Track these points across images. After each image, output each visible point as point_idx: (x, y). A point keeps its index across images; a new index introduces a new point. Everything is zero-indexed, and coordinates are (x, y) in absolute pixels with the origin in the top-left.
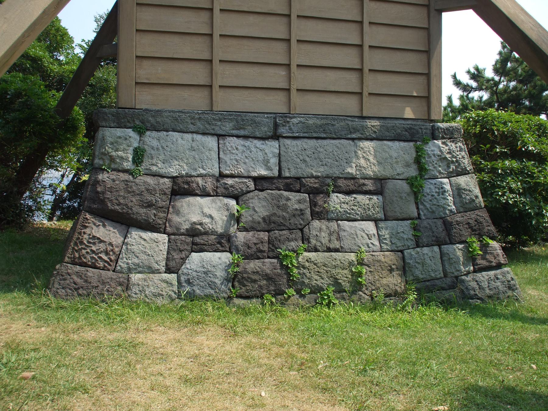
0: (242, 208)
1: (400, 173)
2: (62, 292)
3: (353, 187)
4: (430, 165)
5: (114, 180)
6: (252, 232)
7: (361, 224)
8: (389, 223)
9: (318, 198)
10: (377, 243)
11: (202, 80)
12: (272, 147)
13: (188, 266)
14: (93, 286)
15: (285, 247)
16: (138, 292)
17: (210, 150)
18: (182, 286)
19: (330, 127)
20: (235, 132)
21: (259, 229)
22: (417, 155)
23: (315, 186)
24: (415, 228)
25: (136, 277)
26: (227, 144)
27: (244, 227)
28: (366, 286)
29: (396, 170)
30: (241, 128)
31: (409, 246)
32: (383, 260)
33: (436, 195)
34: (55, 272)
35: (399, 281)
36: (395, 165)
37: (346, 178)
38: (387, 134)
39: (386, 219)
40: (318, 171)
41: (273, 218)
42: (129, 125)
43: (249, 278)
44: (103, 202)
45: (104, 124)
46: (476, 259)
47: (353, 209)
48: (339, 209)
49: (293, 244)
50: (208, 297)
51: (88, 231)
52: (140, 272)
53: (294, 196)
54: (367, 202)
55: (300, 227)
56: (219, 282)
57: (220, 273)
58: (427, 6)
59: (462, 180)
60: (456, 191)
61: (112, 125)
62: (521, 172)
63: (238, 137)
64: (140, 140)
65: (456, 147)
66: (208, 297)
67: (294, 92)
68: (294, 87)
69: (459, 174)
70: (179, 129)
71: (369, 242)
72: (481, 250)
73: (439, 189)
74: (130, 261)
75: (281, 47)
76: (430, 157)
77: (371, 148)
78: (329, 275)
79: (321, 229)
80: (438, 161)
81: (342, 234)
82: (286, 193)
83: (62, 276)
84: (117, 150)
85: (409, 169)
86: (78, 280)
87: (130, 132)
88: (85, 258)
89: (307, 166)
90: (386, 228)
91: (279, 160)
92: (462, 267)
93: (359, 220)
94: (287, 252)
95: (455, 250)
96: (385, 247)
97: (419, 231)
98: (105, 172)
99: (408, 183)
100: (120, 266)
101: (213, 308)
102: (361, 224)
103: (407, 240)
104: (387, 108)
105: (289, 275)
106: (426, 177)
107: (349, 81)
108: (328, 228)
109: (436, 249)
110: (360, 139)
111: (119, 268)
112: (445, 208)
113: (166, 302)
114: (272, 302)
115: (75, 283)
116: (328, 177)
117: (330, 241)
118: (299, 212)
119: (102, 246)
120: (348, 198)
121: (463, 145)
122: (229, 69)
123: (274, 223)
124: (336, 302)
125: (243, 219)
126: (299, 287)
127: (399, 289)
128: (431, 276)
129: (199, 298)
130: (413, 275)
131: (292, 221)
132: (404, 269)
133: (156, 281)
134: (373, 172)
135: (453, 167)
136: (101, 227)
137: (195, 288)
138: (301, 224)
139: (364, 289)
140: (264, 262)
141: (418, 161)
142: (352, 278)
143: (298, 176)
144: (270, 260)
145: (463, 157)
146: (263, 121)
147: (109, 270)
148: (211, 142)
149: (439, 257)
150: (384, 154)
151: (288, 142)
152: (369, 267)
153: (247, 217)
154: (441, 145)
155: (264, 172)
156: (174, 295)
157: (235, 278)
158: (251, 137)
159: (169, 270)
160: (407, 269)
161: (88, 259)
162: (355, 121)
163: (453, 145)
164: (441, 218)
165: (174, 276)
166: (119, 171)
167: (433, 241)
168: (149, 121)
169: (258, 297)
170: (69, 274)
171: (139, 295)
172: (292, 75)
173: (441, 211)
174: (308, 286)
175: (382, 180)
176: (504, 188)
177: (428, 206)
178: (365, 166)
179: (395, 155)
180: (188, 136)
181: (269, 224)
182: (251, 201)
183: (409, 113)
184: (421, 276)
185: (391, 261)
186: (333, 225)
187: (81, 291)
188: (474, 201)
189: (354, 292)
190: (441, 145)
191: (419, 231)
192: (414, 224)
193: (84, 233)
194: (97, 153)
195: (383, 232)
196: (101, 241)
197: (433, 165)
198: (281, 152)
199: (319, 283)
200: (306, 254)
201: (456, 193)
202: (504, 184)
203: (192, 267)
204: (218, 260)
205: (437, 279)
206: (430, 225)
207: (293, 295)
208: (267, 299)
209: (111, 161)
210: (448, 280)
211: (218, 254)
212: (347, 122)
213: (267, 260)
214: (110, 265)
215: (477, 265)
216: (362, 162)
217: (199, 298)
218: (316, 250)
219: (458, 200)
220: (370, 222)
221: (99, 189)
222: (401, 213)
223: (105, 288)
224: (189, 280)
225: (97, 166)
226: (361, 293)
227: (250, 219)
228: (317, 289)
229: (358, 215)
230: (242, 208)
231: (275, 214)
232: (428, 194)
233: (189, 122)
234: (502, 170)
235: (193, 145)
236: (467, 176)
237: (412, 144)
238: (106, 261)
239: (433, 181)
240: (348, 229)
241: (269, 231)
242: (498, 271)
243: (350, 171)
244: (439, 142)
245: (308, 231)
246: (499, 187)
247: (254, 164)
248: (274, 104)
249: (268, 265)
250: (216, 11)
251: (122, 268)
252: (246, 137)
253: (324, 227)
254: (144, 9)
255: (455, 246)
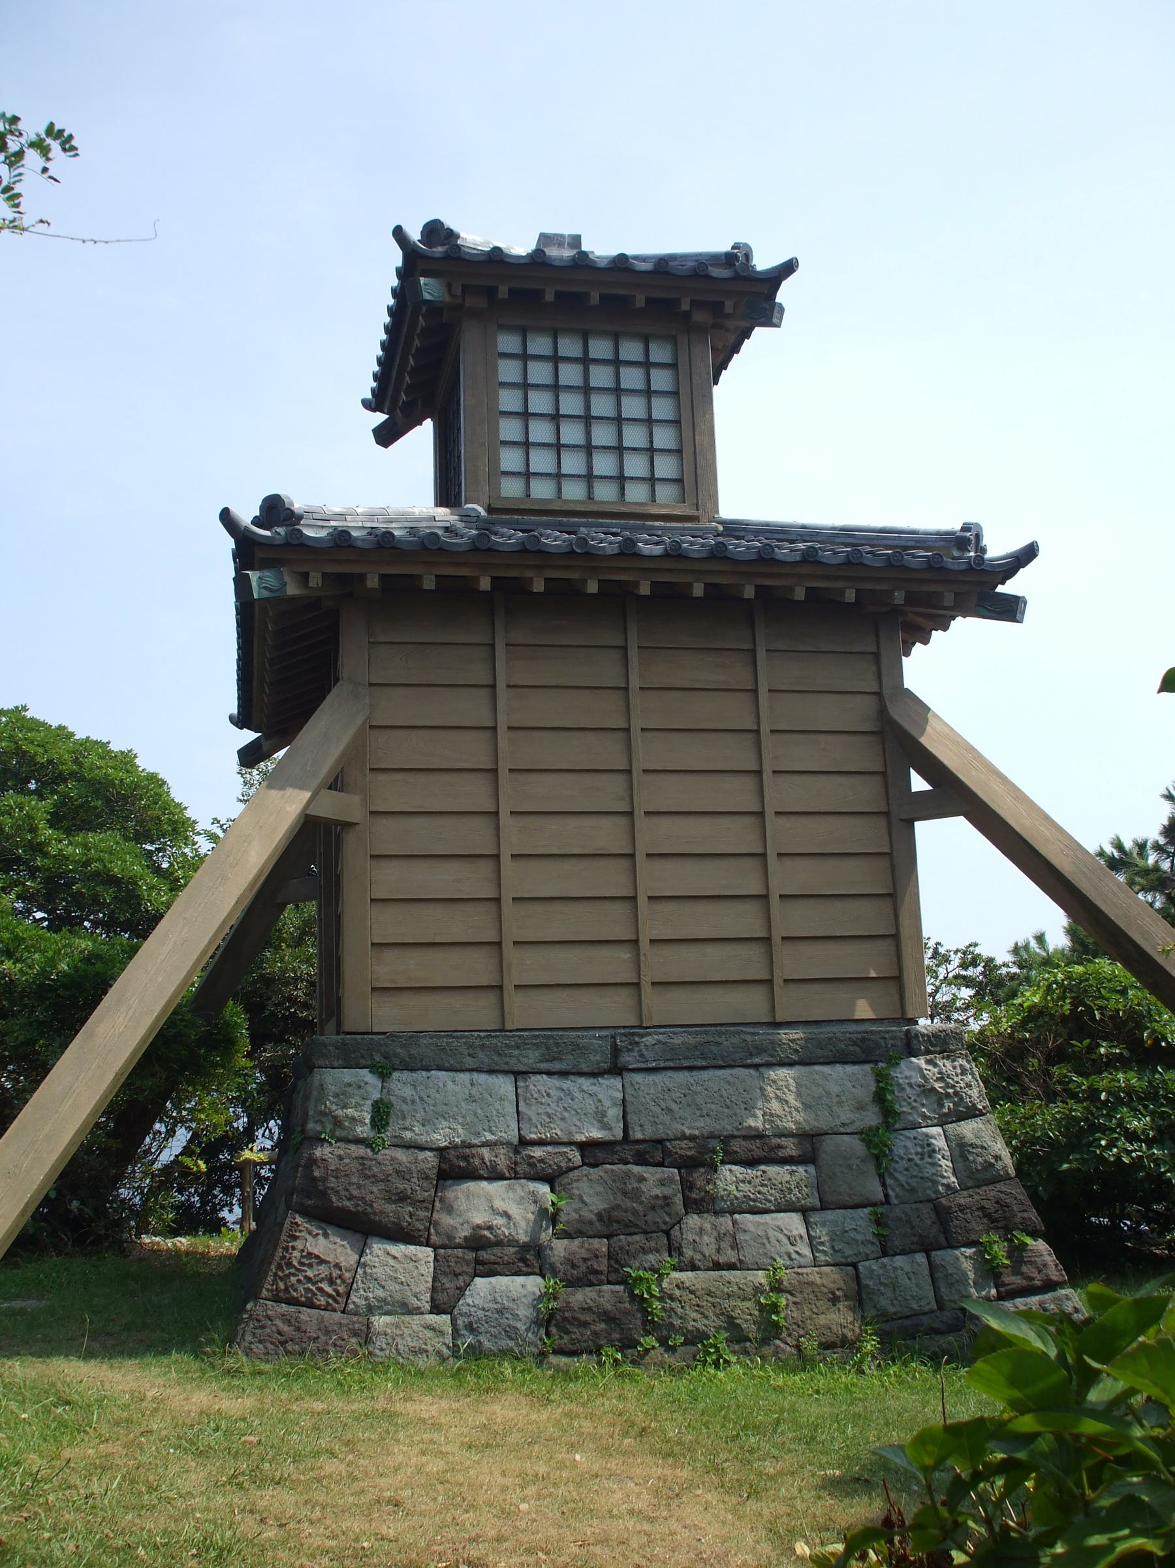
0: (560, 1199)
1: (847, 1121)
2: (258, 1348)
3: (760, 1151)
4: (904, 1103)
5: (341, 1158)
6: (580, 1240)
7: (776, 1219)
8: (829, 1215)
9: (695, 1176)
10: (806, 1251)
11: (486, 977)
12: (609, 1089)
13: (469, 1301)
14: (309, 1338)
15: (637, 1264)
16: (384, 1346)
17: (501, 1099)
18: (460, 1335)
19: (713, 1048)
20: (543, 1066)
21: (591, 1233)
22: (878, 1087)
23: (689, 1153)
24: (879, 1222)
25: (380, 1322)
26: (532, 1087)
27: (565, 1231)
28: (788, 1329)
29: (839, 1117)
30: (554, 1059)
31: (867, 1255)
32: (819, 1281)
33: (916, 1158)
34: (245, 1316)
35: (850, 1319)
36: (835, 1108)
37: (745, 1137)
38: (820, 1052)
39: (823, 1207)
40: (694, 1126)
41: (615, 1214)
42: (363, 1062)
43: (574, 1318)
44: (323, 1194)
45: (321, 1062)
46: (1001, 1273)
47: (759, 1192)
48: (735, 1193)
49: (652, 1258)
50: (504, 1353)
51: (299, 1244)
52: (387, 1313)
53: (652, 1174)
54: (787, 1177)
55: (664, 1227)
56: (523, 1328)
57: (525, 1312)
58: (887, 814)
59: (968, 1129)
60: (957, 1149)
61: (336, 1064)
62: (1151, 1095)
63: (550, 1073)
64: (383, 1087)
65: (954, 1068)
66: (504, 1353)
67: (646, 989)
68: (646, 980)
69: (962, 1117)
70: (447, 1065)
71: (791, 1249)
72: (1007, 1258)
73: (923, 1147)
74: (371, 1295)
75: (620, 910)
76: (904, 1089)
77: (791, 1081)
78: (718, 1311)
79: (701, 1230)
80: (918, 1096)
81: (741, 1237)
82: (637, 1169)
83: (259, 1321)
84: (345, 1106)
85: (864, 1113)
86: (285, 1328)
87: (366, 1075)
88: (296, 1290)
89: (674, 1118)
90: (823, 1224)
91: (624, 1112)
92: (973, 1290)
93: (773, 1212)
94: (641, 1273)
95: (957, 1258)
96: (821, 1257)
97: (887, 1226)
98: (326, 1145)
99: (863, 1140)
100: (354, 1303)
101: (514, 1370)
102: (776, 1219)
103: (863, 1243)
104: (819, 1004)
105: (645, 1312)
106: (897, 1126)
107: (749, 962)
108: (714, 1227)
109: (920, 1258)
110: (769, 1065)
111: (351, 1306)
112: (935, 1183)
113: (433, 1360)
114: (616, 1360)
115: (280, 1333)
116: (712, 1136)
117: (719, 1250)
118: (661, 1202)
119: (323, 1270)
120: (750, 1173)
121: (969, 1062)
122: (531, 957)
123: (617, 1222)
124: (733, 1359)
125: (563, 1217)
126: (665, 1333)
127: (849, 1334)
128: (912, 1309)
129: (489, 1355)
130: (875, 1307)
131: (649, 1217)
132: (859, 1296)
133: (415, 1327)
134: (796, 1122)
135: (948, 1105)
136: (320, 1237)
137: (482, 1338)
138: (665, 1223)
139: (784, 1335)
140: (600, 1291)
141: (880, 1098)
142: (761, 1316)
143: (658, 1137)
144: (612, 1287)
145: (969, 1086)
146: (592, 1044)
147: (335, 1310)
148: (504, 1085)
149: (927, 1272)
150: (815, 1089)
151: (638, 1078)
152: (792, 1295)
153: (569, 1212)
154: (924, 1066)
155: (596, 1134)
156: (445, 1350)
157: (550, 1320)
158: (574, 1074)
159: (436, 1309)
160: (864, 1297)
161: (300, 1292)
162: (758, 1034)
163: (948, 1064)
164: (930, 1201)
165: (446, 1318)
166: (348, 1141)
167: (912, 1243)
168: (397, 1055)
169: (590, 1353)
170: (269, 1318)
171: (387, 1352)
172: (642, 958)
173: (929, 1188)
174: (679, 1331)
175: (813, 1136)
176: (1113, 1130)
177: (902, 1179)
178: (781, 1113)
179: (835, 1089)
180: (464, 1077)
181: (609, 1224)
182: (575, 1185)
183: (863, 1010)
184: (892, 1309)
185: (834, 1282)
186: (725, 1222)
187: (289, 1346)
188: (992, 1165)
189: (765, 1341)
190: (924, 1066)
191: (887, 1226)
192: (876, 1214)
193: (294, 1248)
194: (311, 1113)
195: (817, 1232)
196: (322, 1261)
197: (909, 1104)
198: (627, 1097)
199: (699, 1325)
200: (675, 1275)
201: (957, 1153)
202: (1114, 1121)
203: (477, 1302)
204: (520, 1289)
205: (925, 1314)
206: (907, 1215)
207: (654, 1348)
208: (607, 1356)
209: (335, 1124)
210: (947, 1315)
211: (520, 1280)
212: (743, 1036)
213: (605, 1287)
214: (337, 1302)
215: (1004, 1285)
216: (775, 1106)
217: (489, 1355)
218: (694, 1268)
219: (960, 1165)
220: (793, 1214)
221: (317, 1174)
222: (850, 1195)
223: (336, 1337)
224: (471, 1324)
225: (311, 1134)
226: (778, 1342)
227: (576, 1216)
228: (696, 1337)
229: (770, 1201)
230: (560, 1199)
231: (618, 1206)
232: (902, 1158)
233: (465, 1052)
234: (1109, 1093)
235: (473, 1092)
236: (978, 1119)
237: (868, 1067)
238: (330, 1296)
239: (911, 1134)
240: (752, 1229)
241: (608, 1237)
242: (1048, 1296)
243: (753, 1124)
244: (921, 1062)
245: (678, 1233)
246: (1103, 1129)
247: (579, 1120)
248: (613, 1010)
249: (607, 1295)
250: (505, 859)
251: (357, 1306)
252: (563, 1074)
253: (708, 1226)
254: (384, 863)
255: (957, 1252)
